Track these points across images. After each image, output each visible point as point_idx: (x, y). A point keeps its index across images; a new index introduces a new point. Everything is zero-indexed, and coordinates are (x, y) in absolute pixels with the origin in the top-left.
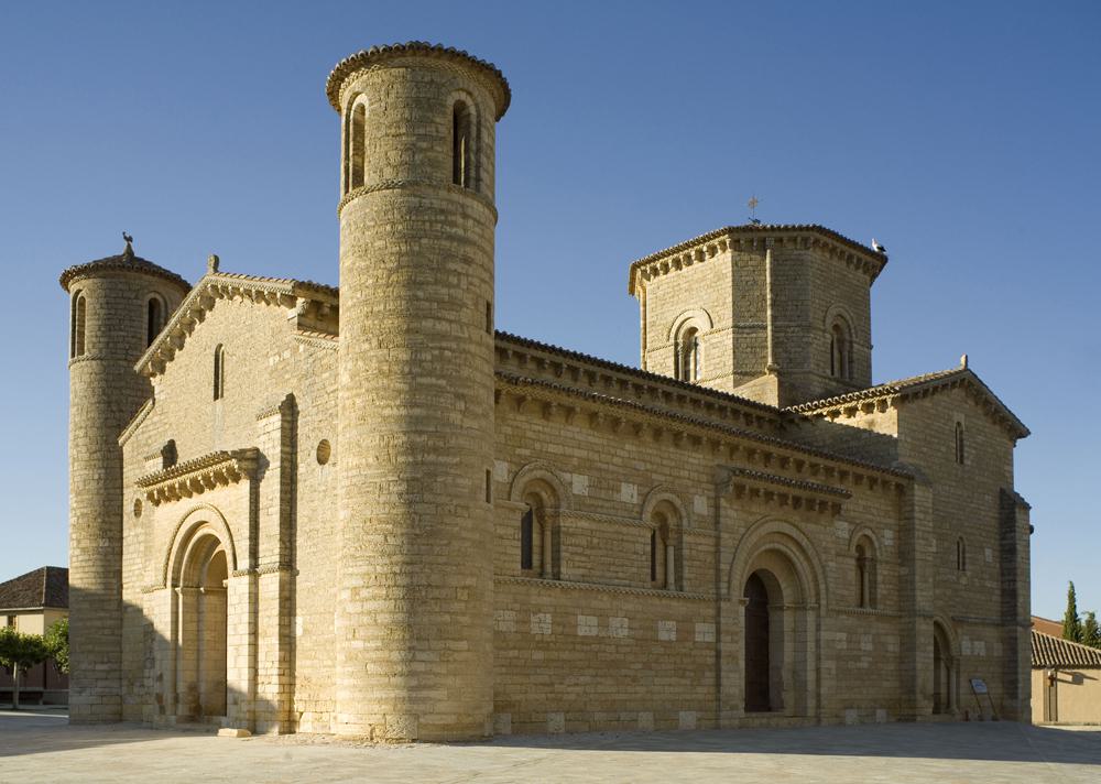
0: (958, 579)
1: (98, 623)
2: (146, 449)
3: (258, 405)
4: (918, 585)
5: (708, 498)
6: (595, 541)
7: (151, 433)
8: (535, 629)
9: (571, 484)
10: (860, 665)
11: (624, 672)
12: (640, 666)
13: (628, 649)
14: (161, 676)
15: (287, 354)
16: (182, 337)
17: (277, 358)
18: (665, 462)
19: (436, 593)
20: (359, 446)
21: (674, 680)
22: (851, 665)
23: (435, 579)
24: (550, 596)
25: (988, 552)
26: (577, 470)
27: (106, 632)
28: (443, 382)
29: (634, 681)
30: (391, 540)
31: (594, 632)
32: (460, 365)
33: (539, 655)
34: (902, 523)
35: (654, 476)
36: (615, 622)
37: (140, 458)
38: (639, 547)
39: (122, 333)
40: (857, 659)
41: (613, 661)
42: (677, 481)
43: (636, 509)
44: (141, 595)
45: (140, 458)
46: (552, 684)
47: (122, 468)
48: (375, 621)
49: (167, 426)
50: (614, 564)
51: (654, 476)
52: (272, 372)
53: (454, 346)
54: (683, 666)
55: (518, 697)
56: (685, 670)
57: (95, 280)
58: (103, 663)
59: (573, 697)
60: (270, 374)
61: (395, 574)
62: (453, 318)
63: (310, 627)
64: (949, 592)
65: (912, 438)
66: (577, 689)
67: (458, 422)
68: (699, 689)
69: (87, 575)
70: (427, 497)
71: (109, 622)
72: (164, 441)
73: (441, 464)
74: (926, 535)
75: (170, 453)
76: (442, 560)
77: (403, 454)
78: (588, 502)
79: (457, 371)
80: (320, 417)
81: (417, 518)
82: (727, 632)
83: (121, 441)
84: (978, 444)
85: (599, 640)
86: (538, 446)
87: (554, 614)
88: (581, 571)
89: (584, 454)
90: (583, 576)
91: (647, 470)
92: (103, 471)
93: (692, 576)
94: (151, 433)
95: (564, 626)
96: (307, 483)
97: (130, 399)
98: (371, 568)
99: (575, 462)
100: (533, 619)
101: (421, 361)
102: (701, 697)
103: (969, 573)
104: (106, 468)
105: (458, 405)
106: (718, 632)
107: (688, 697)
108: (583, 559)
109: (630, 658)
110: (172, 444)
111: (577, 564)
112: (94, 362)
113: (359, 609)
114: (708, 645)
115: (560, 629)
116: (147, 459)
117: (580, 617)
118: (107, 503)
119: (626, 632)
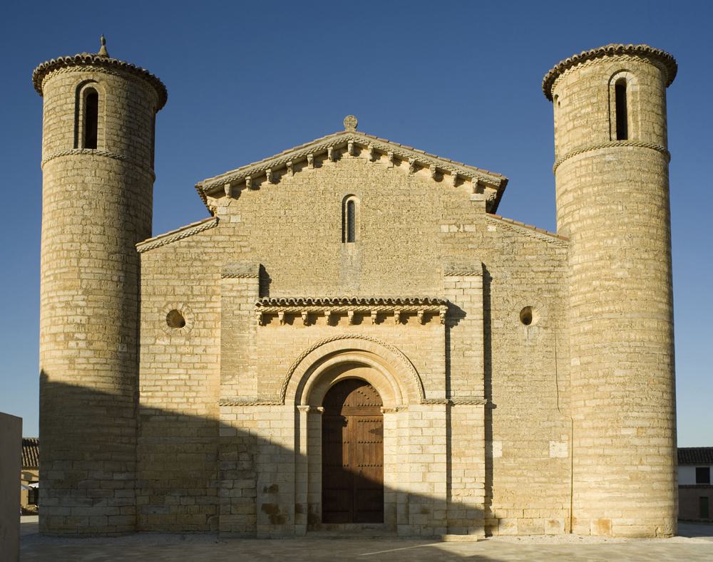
2: (199, 263)
16: (284, 169)
17: (454, 229)
20: (642, 325)
47: (139, 275)
48: (659, 452)
52: (444, 239)
57: (117, 79)
60: (444, 239)
69: (102, 380)
83: (140, 247)
92: (123, 274)
94: (206, 250)
96: (508, 336)
98: (655, 415)
104: (126, 272)
110: (261, 265)
112: (114, 161)
118: (126, 307)
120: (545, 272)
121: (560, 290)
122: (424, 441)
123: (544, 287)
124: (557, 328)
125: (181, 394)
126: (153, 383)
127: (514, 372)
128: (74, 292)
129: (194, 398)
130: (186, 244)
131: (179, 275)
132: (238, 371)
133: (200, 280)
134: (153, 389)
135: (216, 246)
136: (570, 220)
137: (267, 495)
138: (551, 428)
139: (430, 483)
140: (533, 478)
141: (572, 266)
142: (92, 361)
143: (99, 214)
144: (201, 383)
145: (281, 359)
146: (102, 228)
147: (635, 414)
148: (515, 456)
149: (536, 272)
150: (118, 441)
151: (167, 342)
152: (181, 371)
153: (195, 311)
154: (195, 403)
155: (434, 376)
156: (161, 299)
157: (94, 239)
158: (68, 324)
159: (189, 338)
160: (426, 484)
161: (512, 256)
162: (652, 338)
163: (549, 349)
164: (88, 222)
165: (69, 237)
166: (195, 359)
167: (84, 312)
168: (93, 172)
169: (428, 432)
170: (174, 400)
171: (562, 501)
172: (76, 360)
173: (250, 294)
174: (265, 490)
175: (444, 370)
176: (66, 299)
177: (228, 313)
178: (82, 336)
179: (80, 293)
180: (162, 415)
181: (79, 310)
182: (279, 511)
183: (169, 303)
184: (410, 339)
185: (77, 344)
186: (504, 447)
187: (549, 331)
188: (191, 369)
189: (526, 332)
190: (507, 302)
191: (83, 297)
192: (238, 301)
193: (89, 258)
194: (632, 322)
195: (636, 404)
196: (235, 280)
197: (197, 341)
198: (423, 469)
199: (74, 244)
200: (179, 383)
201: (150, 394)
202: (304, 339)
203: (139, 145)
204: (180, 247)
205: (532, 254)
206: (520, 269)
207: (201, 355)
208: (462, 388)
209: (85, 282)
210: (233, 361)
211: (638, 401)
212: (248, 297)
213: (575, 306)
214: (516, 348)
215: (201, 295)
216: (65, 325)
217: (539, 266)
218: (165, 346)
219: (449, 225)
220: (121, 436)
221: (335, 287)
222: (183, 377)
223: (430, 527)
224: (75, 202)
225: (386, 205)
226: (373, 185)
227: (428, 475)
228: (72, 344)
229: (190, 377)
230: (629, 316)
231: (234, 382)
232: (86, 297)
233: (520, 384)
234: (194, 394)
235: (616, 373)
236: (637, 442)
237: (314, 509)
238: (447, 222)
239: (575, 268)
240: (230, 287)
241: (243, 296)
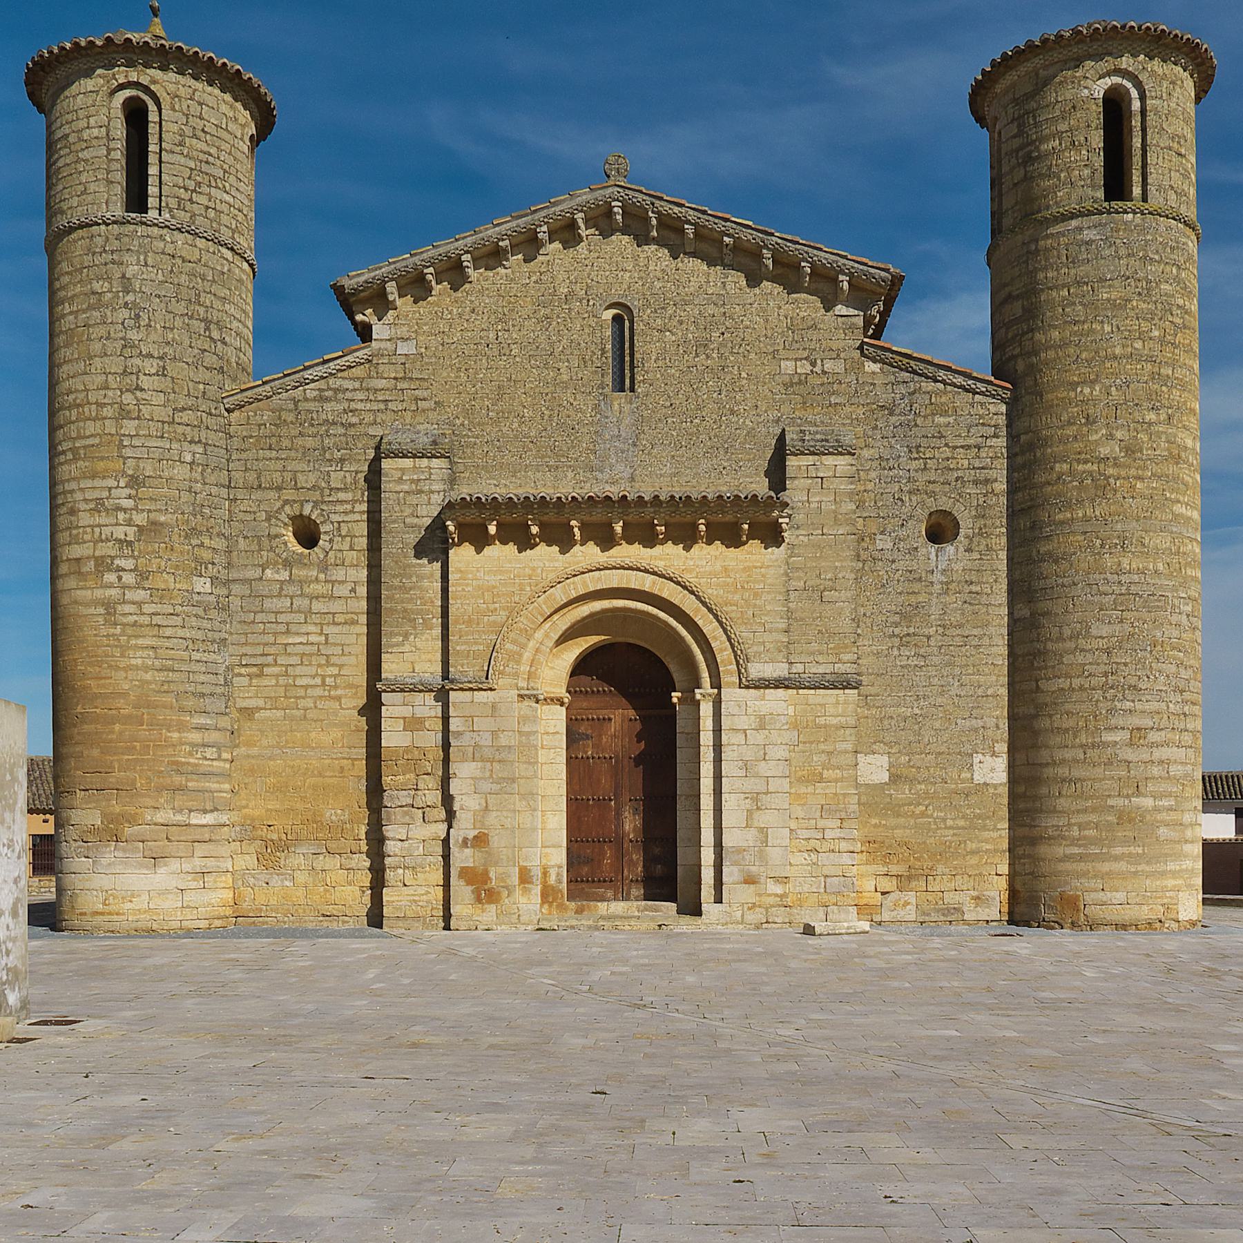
2: (341, 430)
94: (353, 405)
96: (900, 565)
113: (1146, 757)
120: (969, 447)
121: (996, 480)
122: (749, 754)
123: (969, 475)
124: (989, 548)
125: (313, 671)
126: (259, 650)
127: (912, 630)
128: (111, 483)
129: (335, 676)
130: (316, 393)
131: (306, 451)
132: (415, 628)
133: (342, 460)
134: (259, 661)
135: (371, 397)
136: (1017, 351)
137: (468, 851)
138: (976, 730)
139: (761, 830)
140: (944, 820)
141: (1018, 436)
142: (148, 609)
143: (153, 337)
144: (346, 650)
145: (492, 607)
146: (161, 364)
147: (1129, 705)
148: (912, 781)
149: (955, 448)
150: (199, 756)
151: (284, 575)
152: (312, 628)
153: (334, 518)
154: (336, 687)
155: (767, 637)
156: (272, 494)
157: (145, 382)
158: (102, 541)
159: (324, 567)
160: (753, 831)
161: (911, 417)
162: (1160, 566)
163: (974, 588)
164: (135, 352)
165: (100, 379)
166: (337, 606)
167: (131, 519)
168: (142, 258)
169: (758, 738)
170: (299, 682)
171: (996, 860)
172: (119, 608)
173: (435, 487)
174: (465, 840)
176: (96, 494)
177: (394, 522)
178: (128, 564)
179: (122, 484)
180: (276, 709)
181: (121, 516)
182: (490, 879)
183: (286, 502)
184: (726, 569)
185: (120, 578)
186: (891, 765)
187: (976, 555)
188: (328, 624)
189: (933, 556)
190: (900, 503)
191: (128, 491)
192: (413, 499)
193: (138, 418)
194: (1125, 538)
195: (1130, 686)
196: (407, 463)
197: (339, 574)
198: (748, 804)
199: (110, 393)
200: (308, 649)
201: (255, 670)
202: (534, 569)
203: (224, 208)
204: (306, 400)
205: (945, 413)
206: (924, 442)
207: (346, 598)
208: (820, 659)
209: (130, 462)
210: (405, 610)
211: (1133, 681)
212: (432, 492)
213: (1023, 509)
214: (916, 587)
215: (345, 489)
216: (95, 543)
217: (959, 436)
218: (282, 582)
219: (796, 360)
220: (204, 745)
221: (588, 475)
222: (313, 638)
223: (760, 906)
224: (109, 314)
225: (681, 323)
226: (658, 284)
227: (756, 815)
228: (111, 577)
229: (327, 639)
230: (1119, 526)
231: (407, 648)
232: (133, 492)
233: (922, 651)
234: (335, 671)
235: (1094, 632)
236: (1129, 754)
237: (552, 880)
238: (792, 355)
239: (1023, 438)
240: (398, 474)
241: (420, 492)
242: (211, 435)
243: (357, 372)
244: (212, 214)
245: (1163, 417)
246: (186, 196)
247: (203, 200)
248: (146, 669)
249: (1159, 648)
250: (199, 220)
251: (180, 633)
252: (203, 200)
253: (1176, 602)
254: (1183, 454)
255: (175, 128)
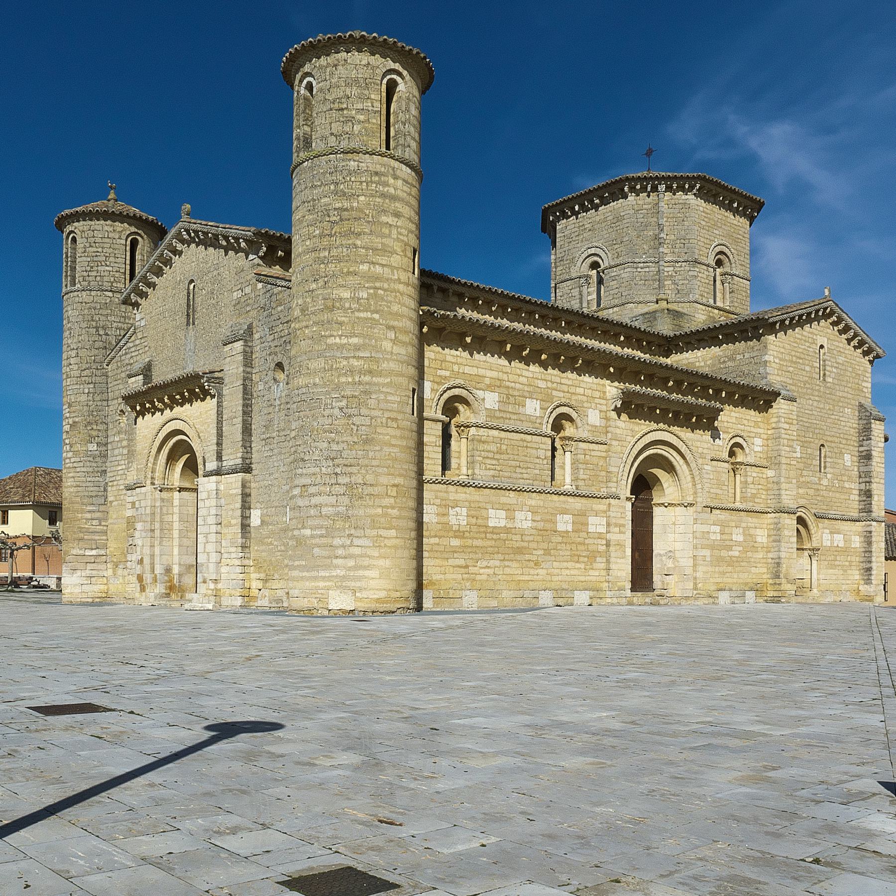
0: (820, 479)
1: (88, 516)
2: (129, 367)
3: (225, 332)
4: (784, 486)
5: (601, 411)
6: (504, 447)
7: (133, 354)
8: (453, 520)
9: (484, 399)
10: (731, 553)
11: (527, 557)
12: (542, 552)
13: (531, 538)
14: (142, 559)
15: (248, 290)
18: (563, 381)
19: (370, 490)
21: (570, 565)
22: (724, 553)
23: (370, 478)
24: (466, 493)
25: (847, 457)
26: (490, 388)
27: (94, 522)
28: (376, 316)
29: (535, 565)
30: (335, 447)
31: (503, 523)
32: (391, 302)
33: (455, 542)
34: (769, 432)
35: (554, 393)
36: (519, 515)
37: (123, 375)
38: (541, 453)
39: (107, 268)
40: (729, 548)
41: (518, 548)
42: (574, 397)
43: (538, 421)
44: (124, 492)
45: (123, 375)
46: (467, 567)
49: (147, 349)
50: (519, 467)
51: (554, 393)
53: (386, 286)
54: (578, 553)
55: (438, 577)
56: (579, 556)
58: (92, 549)
59: (484, 577)
61: (336, 474)
62: (384, 262)
63: (266, 519)
64: (811, 492)
65: (781, 360)
66: (490, 571)
67: (389, 349)
68: (591, 572)
70: (364, 411)
71: (98, 515)
72: (147, 360)
73: (375, 384)
74: (790, 443)
75: (147, 371)
76: (374, 463)
77: (345, 374)
78: (498, 414)
79: (388, 307)
80: (276, 343)
81: (355, 428)
82: (616, 525)
84: (838, 363)
85: (507, 530)
86: (456, 368)
87: (469, 508)
88: (492, 473)
89: (494, 374)
90: (493, 476)
91: (548, 388)
93: (585, 477)
94: (133, 354)
95: (477, 518)
96: (265, 398)
97: (115, 325)
98: (318, 469)
99: (487, 381)
100: (451, 512)
101: (359, 299)
102: (594, 579)
103: (829, 476)
105: (388, 335)
106: (608, 525)
107: (582, 578)
108: (494, 462)
109: (533, 545)
111: (488, 466)
114: (600, 536)
115: (474, 521)
116: (130, 376)
117: (490, 511)
119: (529, 524)
175: (215, 441)
211: (302, 455)
242: (98, 378)
243: (133, 338)
244: (98, 278)
245: (321, 283)
246: (85, 274)
247: (94, 274)
248: (72, 486)
249: (315, 432)
250: (92, 283)
251: (83, 469)
252: (94, 274)
253: (329, 401)
254: (338, 305)
255: (82, 245)
